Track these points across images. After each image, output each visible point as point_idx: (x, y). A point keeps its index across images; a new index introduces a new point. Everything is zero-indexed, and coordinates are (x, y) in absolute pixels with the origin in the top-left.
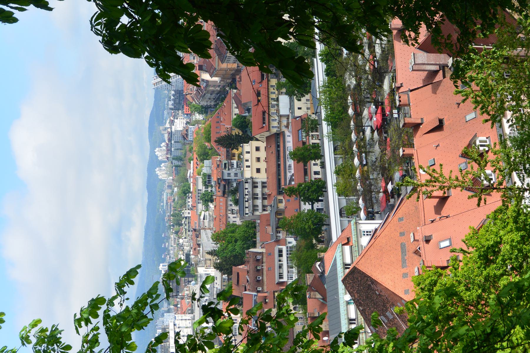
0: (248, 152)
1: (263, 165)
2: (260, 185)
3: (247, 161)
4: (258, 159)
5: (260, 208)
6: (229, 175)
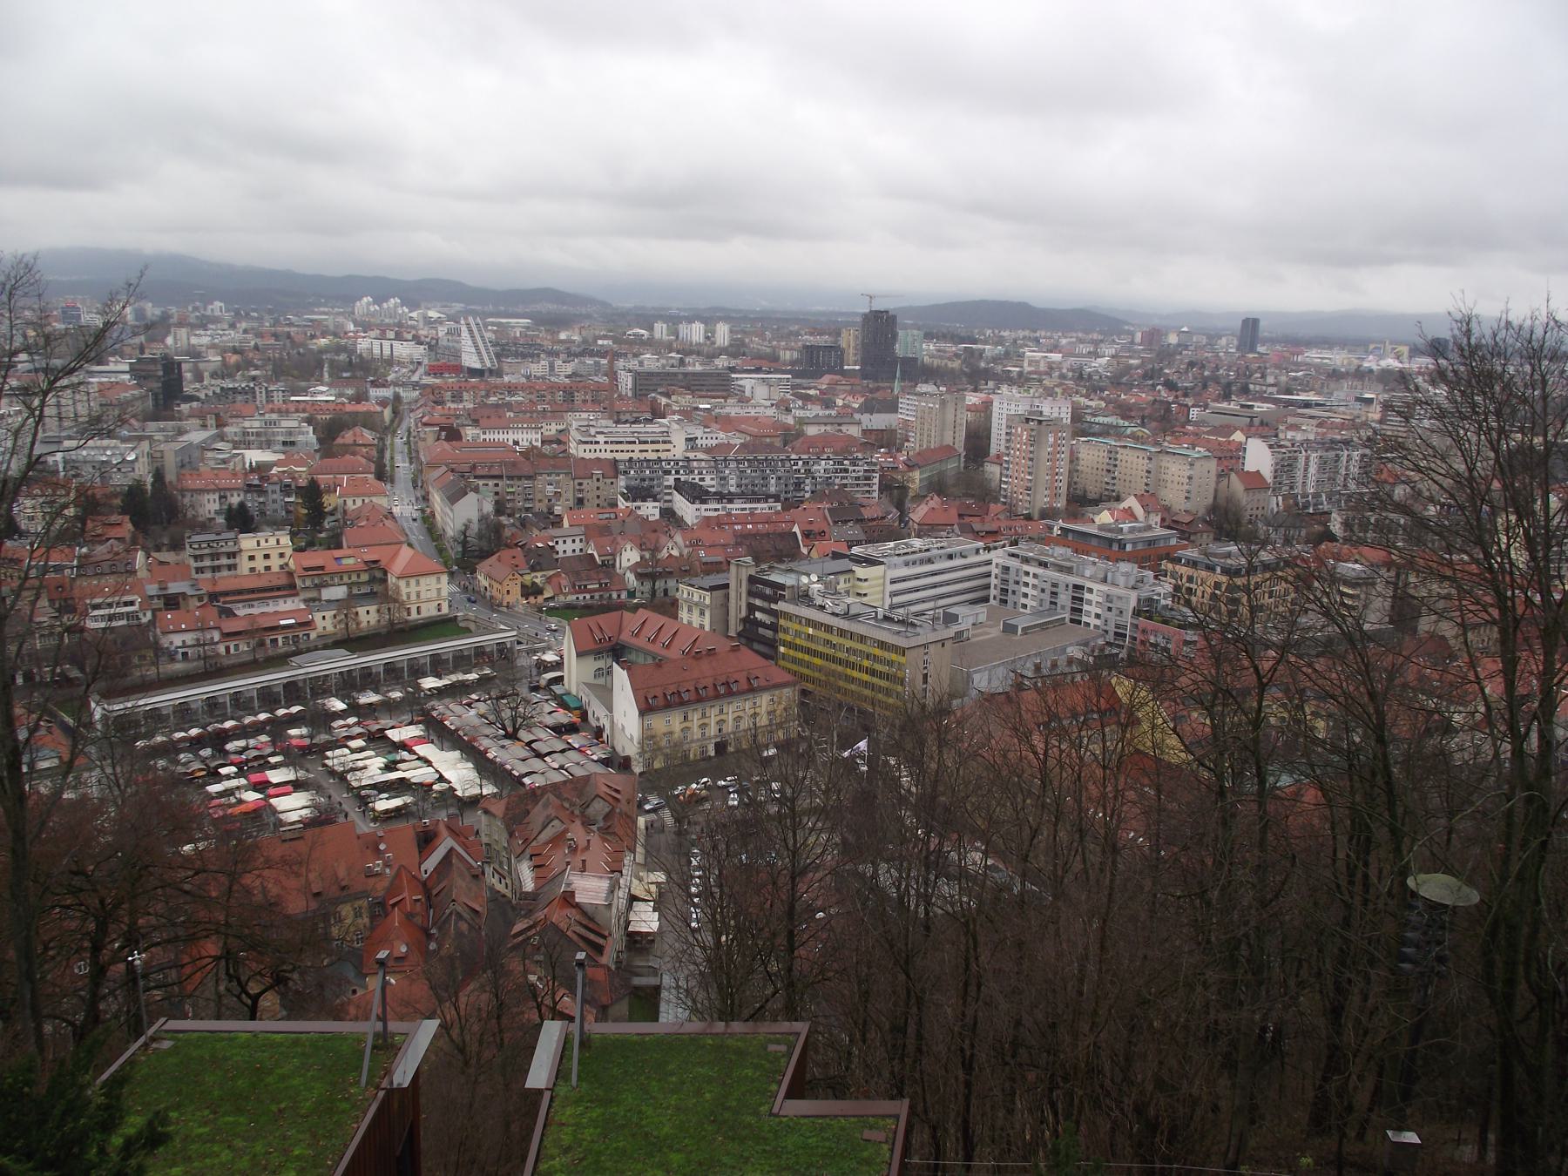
2: (231, 561)
4: (267, 557)
5: (200, 564)
6: (274, 492)
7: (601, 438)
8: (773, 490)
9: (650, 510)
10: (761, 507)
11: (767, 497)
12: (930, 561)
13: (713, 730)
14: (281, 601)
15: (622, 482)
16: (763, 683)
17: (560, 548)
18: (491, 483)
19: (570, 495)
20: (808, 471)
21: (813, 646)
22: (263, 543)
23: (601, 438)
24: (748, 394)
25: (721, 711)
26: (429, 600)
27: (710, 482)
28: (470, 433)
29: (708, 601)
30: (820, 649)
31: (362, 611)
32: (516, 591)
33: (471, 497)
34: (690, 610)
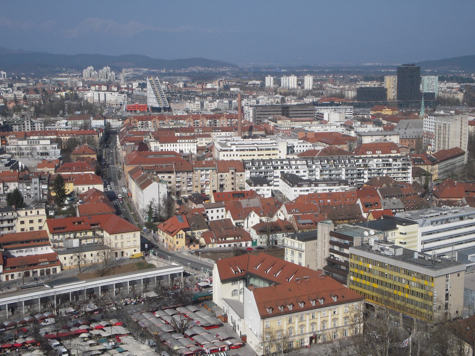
0: (38, 212)
1: (27, 226)
3: (31, 212)
4: (31, 222)
6: (35, 183)
7: (234, 148)
8: (344, 177)
9: (265, 191)
10: (336, 189)
11: (341, 182)
12: (447, 221)
13: (307, 329)
14: (39, 248)
15: (247, 175)
16: (341, 299)
17: (209, 215)
18: (166, 176)
19: (215, 182)
20: (366, 166)
21: (372, 276)
22: (29, 212)
23: (234, 148)
24: (326, 118)
25: (313, 317)
26: (129, 248)
27: (303, 173)
28: (154, 146)
29: (304, 248)
30: (377, 277)
31: (88, 254)
32: (182, 242)
33: (155, 184)
34: (293, 253)
